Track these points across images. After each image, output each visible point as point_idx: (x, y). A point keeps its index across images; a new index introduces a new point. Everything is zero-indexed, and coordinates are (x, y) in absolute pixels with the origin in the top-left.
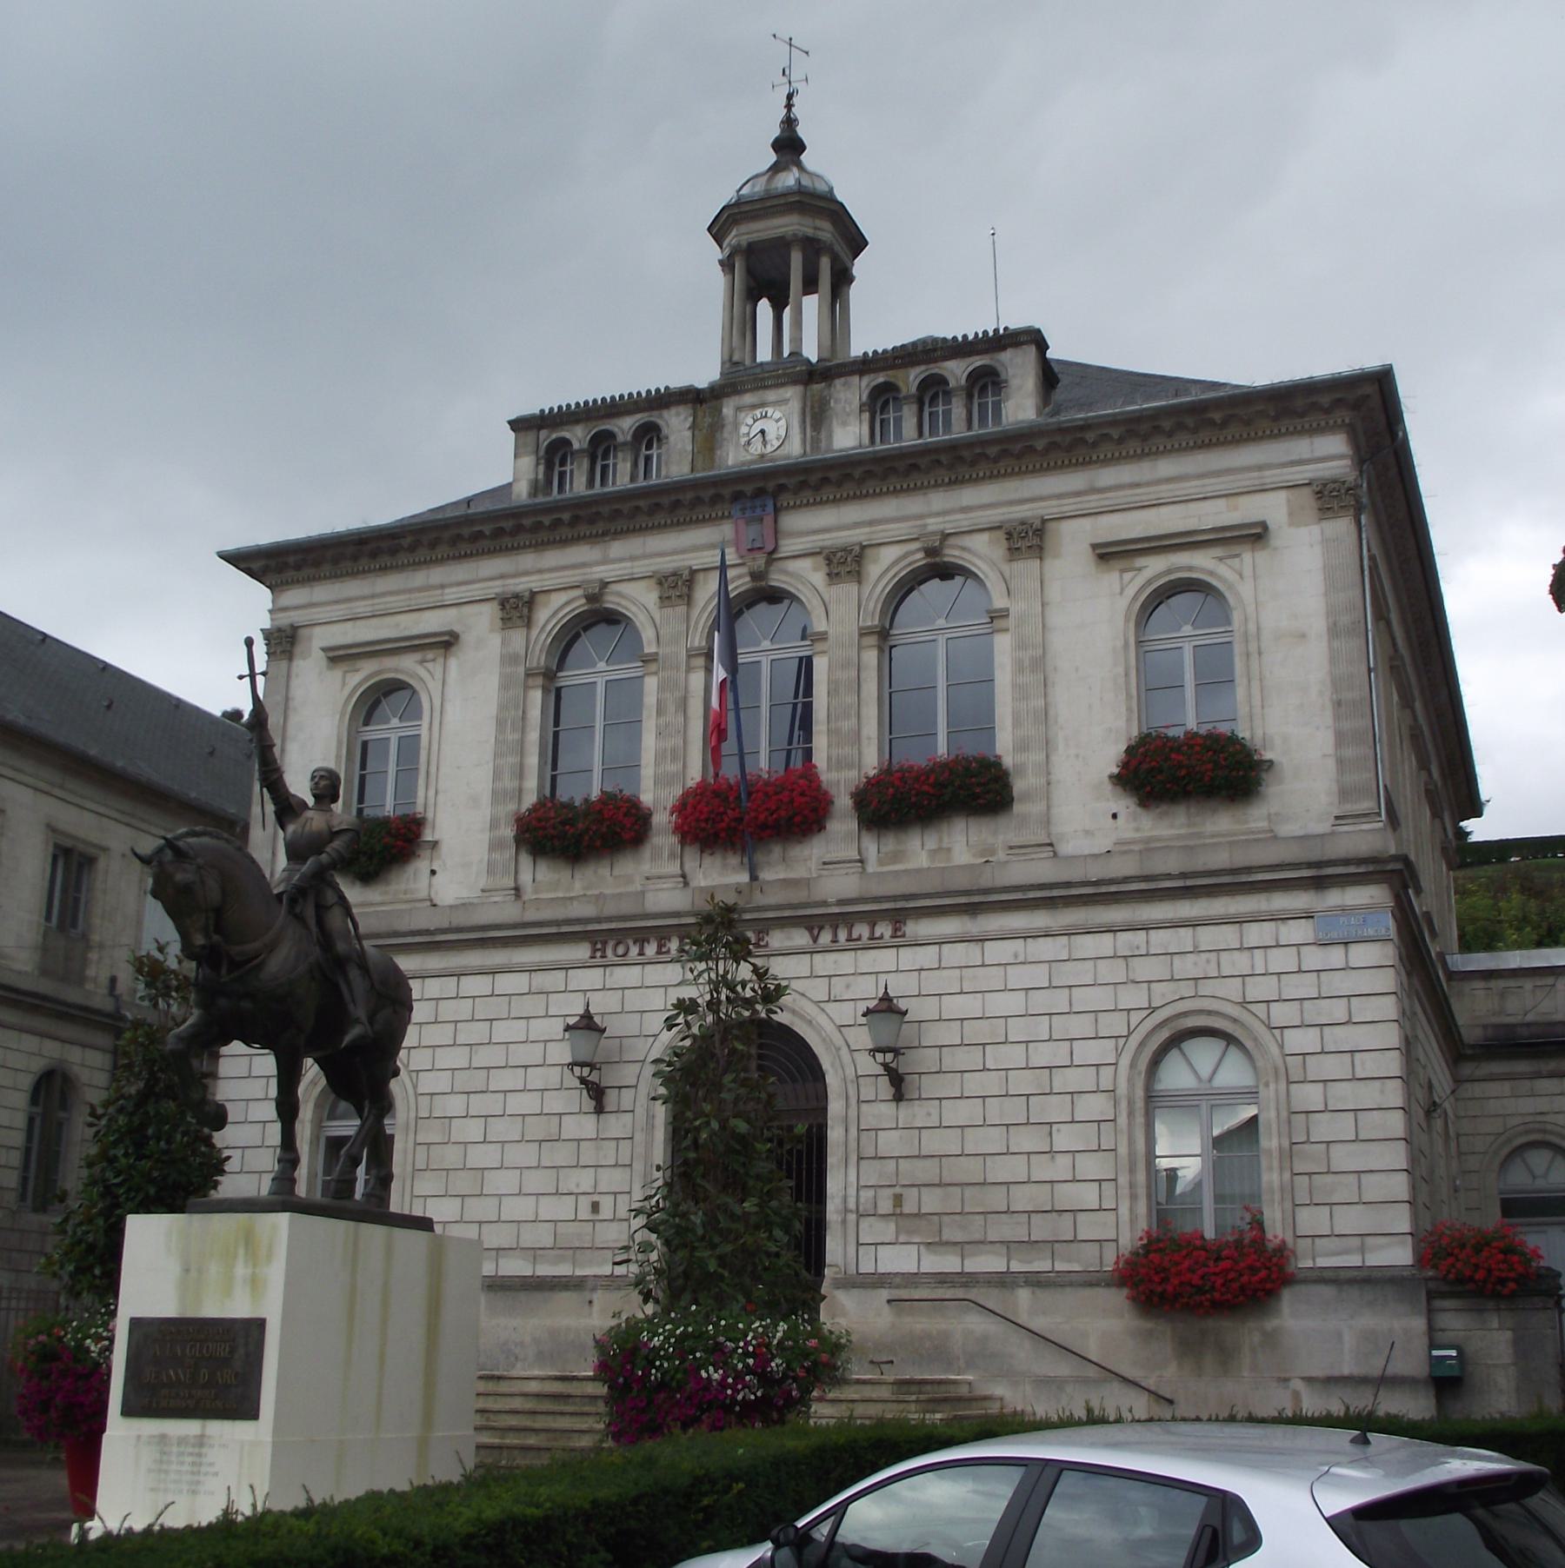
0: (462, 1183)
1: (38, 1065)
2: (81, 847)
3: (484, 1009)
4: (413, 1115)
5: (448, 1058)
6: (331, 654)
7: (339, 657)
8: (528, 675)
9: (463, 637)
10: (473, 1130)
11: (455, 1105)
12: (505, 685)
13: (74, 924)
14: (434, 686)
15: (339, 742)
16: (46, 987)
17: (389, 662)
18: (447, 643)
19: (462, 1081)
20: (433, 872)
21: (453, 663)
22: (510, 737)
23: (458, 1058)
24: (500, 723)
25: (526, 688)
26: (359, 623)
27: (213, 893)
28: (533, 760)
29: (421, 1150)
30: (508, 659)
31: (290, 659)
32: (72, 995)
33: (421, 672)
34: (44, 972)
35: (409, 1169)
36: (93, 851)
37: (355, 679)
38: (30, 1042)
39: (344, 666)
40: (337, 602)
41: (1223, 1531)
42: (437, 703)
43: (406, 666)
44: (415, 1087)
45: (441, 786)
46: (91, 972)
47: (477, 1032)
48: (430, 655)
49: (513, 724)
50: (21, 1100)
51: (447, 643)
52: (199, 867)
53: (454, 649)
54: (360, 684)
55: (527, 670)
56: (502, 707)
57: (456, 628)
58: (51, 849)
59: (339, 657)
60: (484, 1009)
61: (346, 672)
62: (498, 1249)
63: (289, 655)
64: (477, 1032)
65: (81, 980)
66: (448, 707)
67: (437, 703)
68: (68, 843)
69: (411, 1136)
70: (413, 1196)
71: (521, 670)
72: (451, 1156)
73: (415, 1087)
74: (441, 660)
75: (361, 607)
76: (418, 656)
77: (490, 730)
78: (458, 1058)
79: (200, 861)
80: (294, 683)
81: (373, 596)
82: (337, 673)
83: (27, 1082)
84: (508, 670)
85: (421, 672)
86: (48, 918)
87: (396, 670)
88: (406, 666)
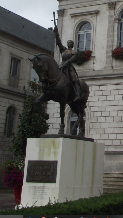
0: (100, 131)
1: (8, 105)
2: (17, 58)
4: (89, 116)
5: (97, 104)
6: (72, 15)
7: (74, 16)
8: (115, 20)
10: (103, 119)
11: (99, 114)
12: (110, 22)
13: (16, 74)
14: (94, 22)
15: (74, 35)
16: (10, 88)
18: (97, 13)
20: (94, 63)
21: (98, 17)
23: (99, 104)
24: (109, 30)
25: (114, 23)
26: (78, 9)
27: (46, 68)
28: (116, 39)
29: (91, 124)
30: (110, 17)
31: (63, 16)
32: (15, 90)
33: (91, 19)
34: (9, 85)
35: (89, 128)
36: (20, 58)
37: (77, 21)
38: (6, 100)
39: (74, 18)
40: (73, 4)
42: (95, 26)
43: (88, 18)
44: (90, 110)
45: (96, 44)
46: (20, 85)
47: (103, 98)
48: (93, 16)
50: (4, 113)
51: (97, 13)
52: (43, 62)
53: (98, 14)
54: (78, 22)
55: (114, 19)
56: (109, 27)
57: (99, 10)
58: (11, 58)
59: (74, 16)
61: (75, 19)
62: (108, 146)
63: (63, 16)
64: (103, 98)
65: (17, 87)
66: (97, 27)
67: (95, 26)
68: (15, 57)
69: (89, 121)
70: (89, 134)
71: (113, 19)
72: (98, 125)
73: (90, 110)
74: (96, 17)
78: (99, 104)
79: (43, 61)
80: (64, 22)
81: (81, 3)
82: (73, 20)
83: (6, 109)
84: (110, 19)
85: (91, 19)
86: (10, 73)
87: (86, 19)
88: (88, 18)
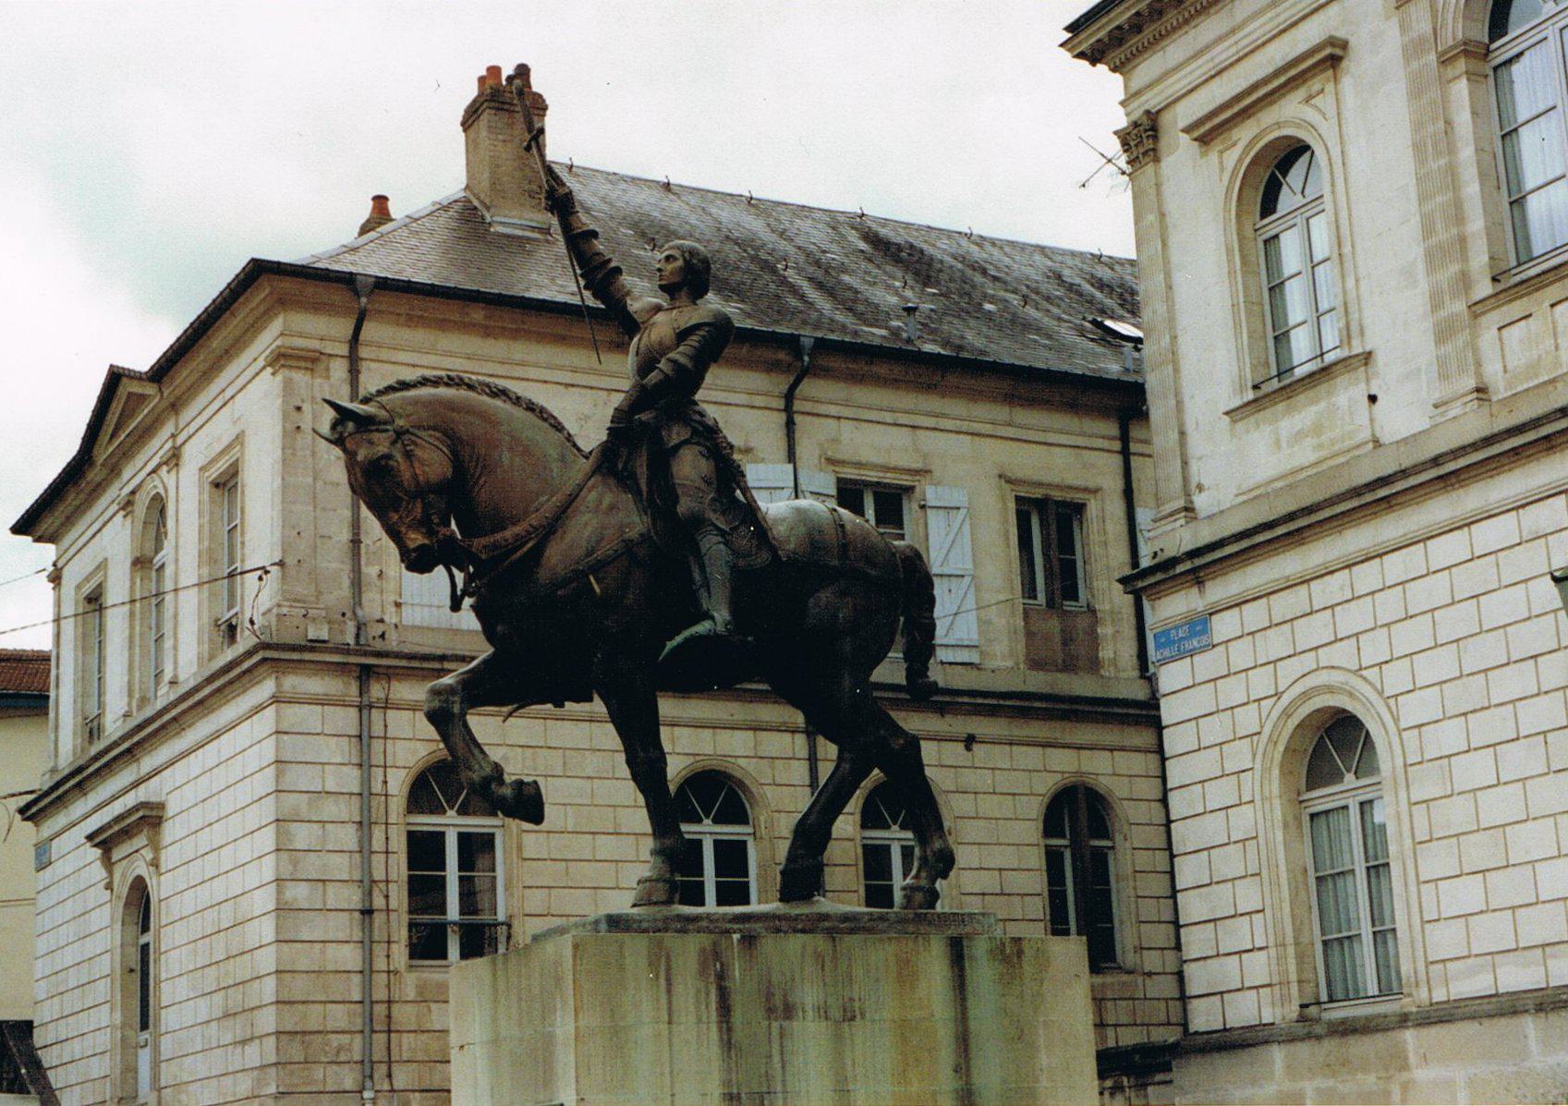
0: (1479, 851)
1: (1047, 785)
2: (1058, 495)
3: (1469, 579)
4: (1399, 762)
5: (1430, 668)
6: (1196, 134)
7: (1209, 132)
8: (1445, 61)
9: (1353, 42)
10: (1477, 769)
11: (1449, 736)
12: (1416, 92)
13: (1071, 593)
14: (1328, 129)
15: (1229, 251)
16: (1037, 682)
17: (1268, 117)
18: (1331, 57)
19: (1459, 696)
20: (1373, 399)
21: (1347, 83)
22: (1435, 166)
23: (1439, 665)
24: (1418, 148)
25: (1445, 83)
26: (1225, 75)
27: (432, 462)
28: (1472, 189)
29: (1419, 812)
30: (1412, 50)
31: (1157, 160)
32: (1081, 685)
33: (1309, 114)
34: (1036, 664)
35: (1408, 842)
36: (1078, 497)
37: (1232, 156)
38: (1030, 756)
39: (1218, 145)
40: (1195, 57)
41: (1299, 1097)
42: (1335, 152)
43: (1289, 116)
44: (1396, 720)
45: (1362, 272)
46: (1106, 653)
47: (1456, 622)
48: (1315, 85)
49: (1435, 144)
50: (1031, 831)
51: (1331, 57)
52: (400, 434)
53: (1344, 64)
54: (1240, 160)
55: (1440, 55)
56: (1418, 126)
57: (1341, 34)
58: (1012, 505)
59: (1209, 132)
60: (1469, 579)
61: (1221, 152)
63: (1154, 155)
64: (1456, 622)
65: (1094, 665)
66: (1352, 154)
67: (1335, 152)
68: (1038, 493)
69: (1403, 795)
70: (1419, 883)
71: (1432, 57)
72: (1456, 814)
73: (1396, 720)
74: (1330, 87)
75: (1223, 53)
76: (1301, 93)
77: (1407, 164)
78: (1439, 665)
79: (400, 422)
80: (1167, 190)
81: (1233, 31)
82: (1213, 157)
83: (1034, 809)
84: (1415, 65)
85: (1309, 114)
86: (1030, 591)
87: (1278, 125)
88: (1289, 116)
